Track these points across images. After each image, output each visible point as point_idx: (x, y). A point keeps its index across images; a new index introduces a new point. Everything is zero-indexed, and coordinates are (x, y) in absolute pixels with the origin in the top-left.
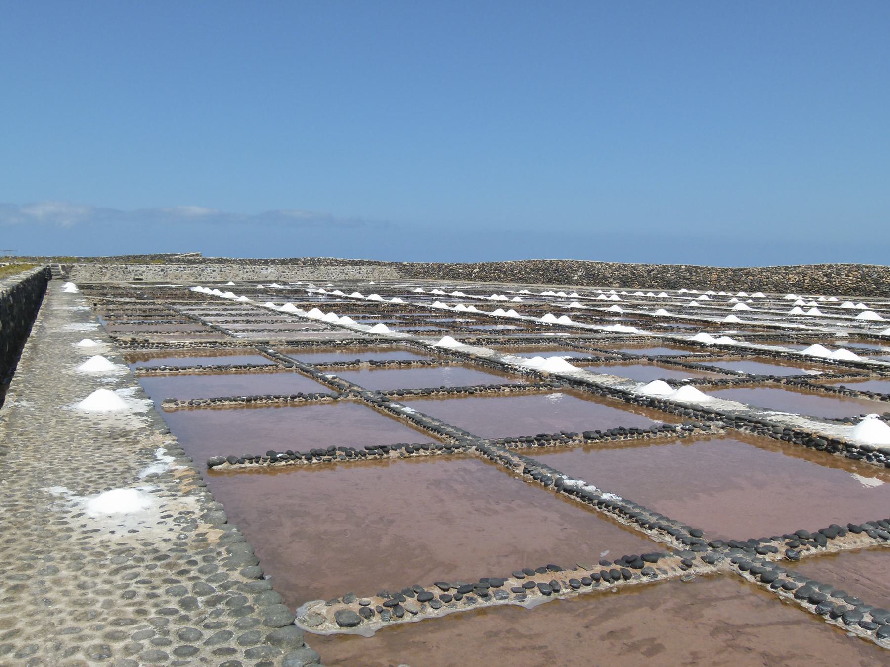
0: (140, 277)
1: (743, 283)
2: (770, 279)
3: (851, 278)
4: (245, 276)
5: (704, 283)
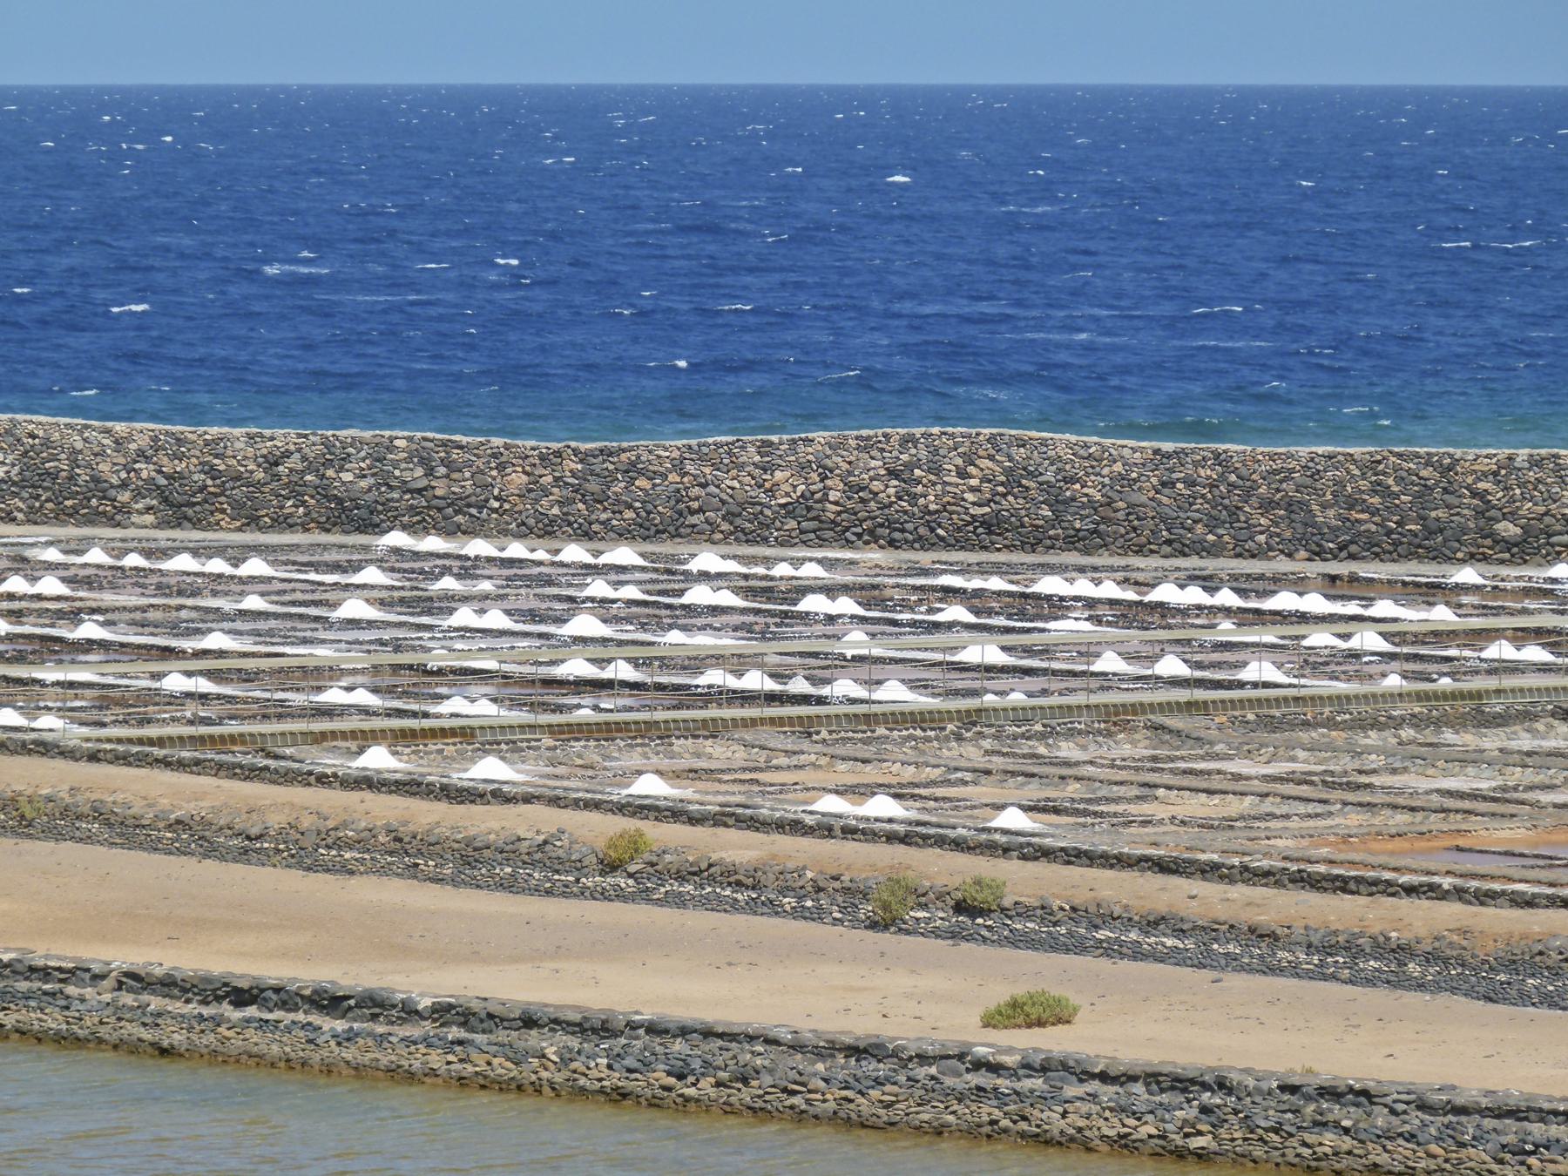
1: (619, 505)
2: (712, 489)
3: (974, 482)
5: (480, 508)
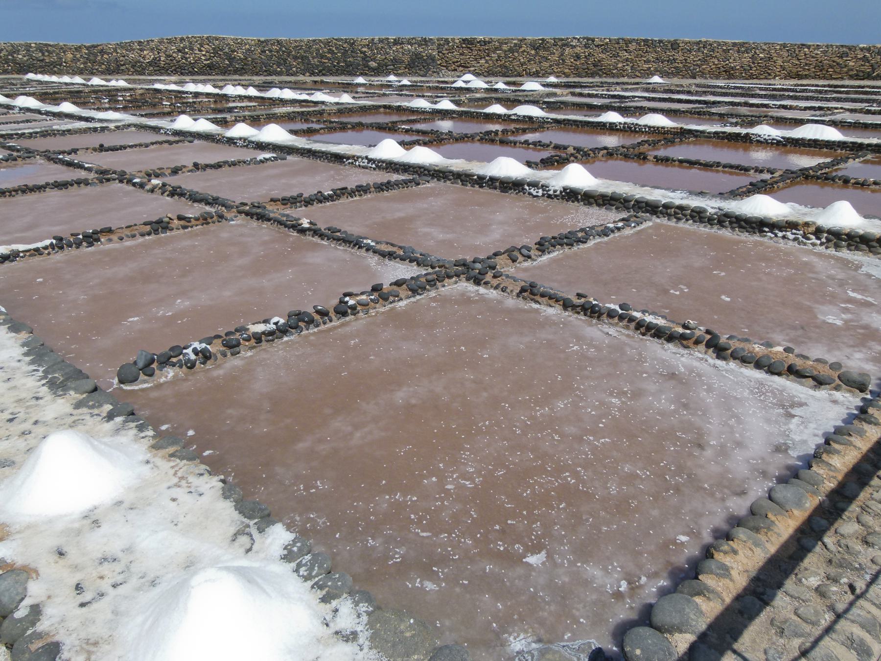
3: (204, 53)
5: (61, 65)
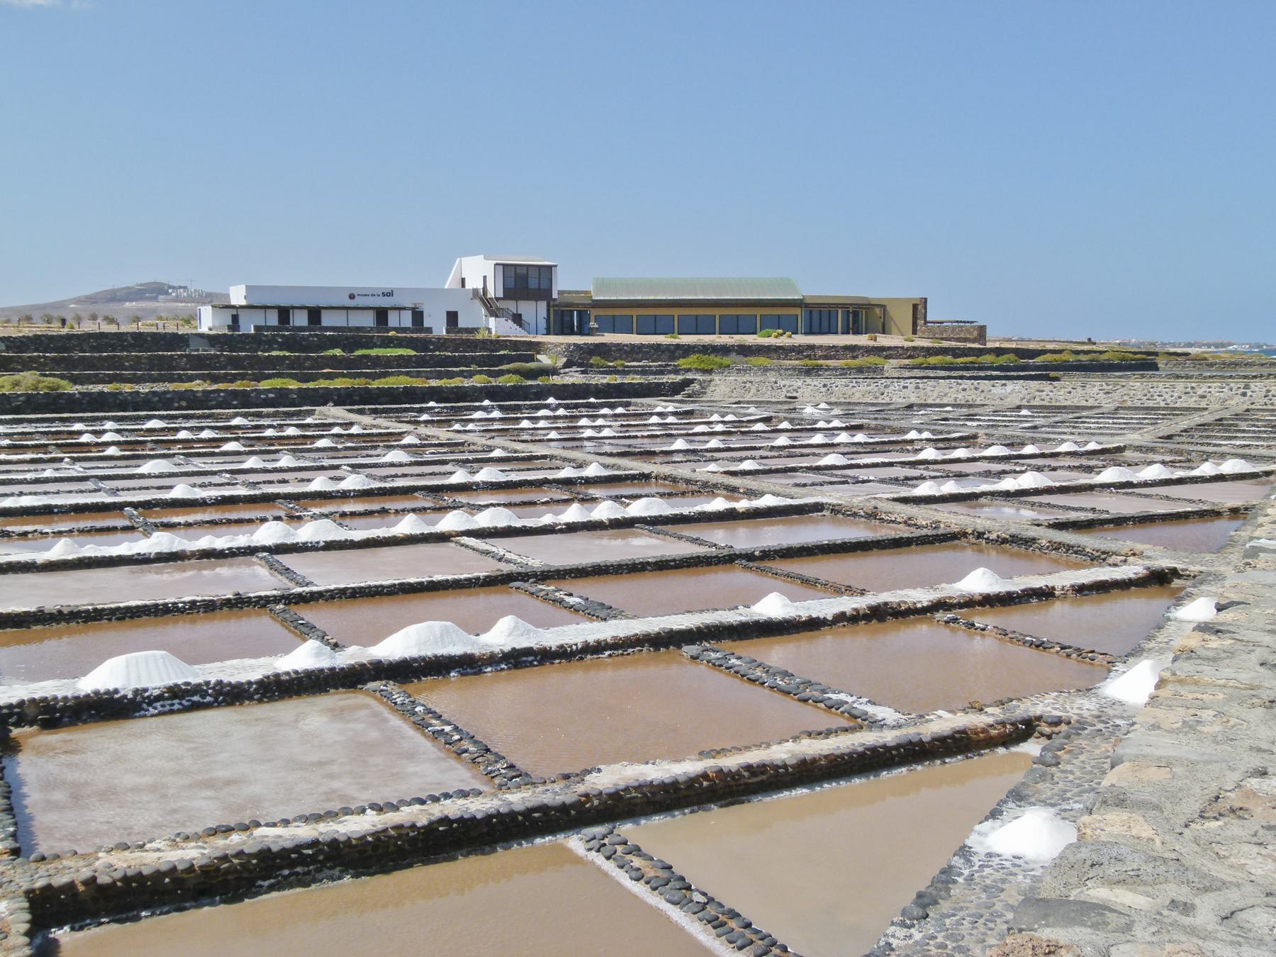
0: (794, 394)
4: (960, 396)
